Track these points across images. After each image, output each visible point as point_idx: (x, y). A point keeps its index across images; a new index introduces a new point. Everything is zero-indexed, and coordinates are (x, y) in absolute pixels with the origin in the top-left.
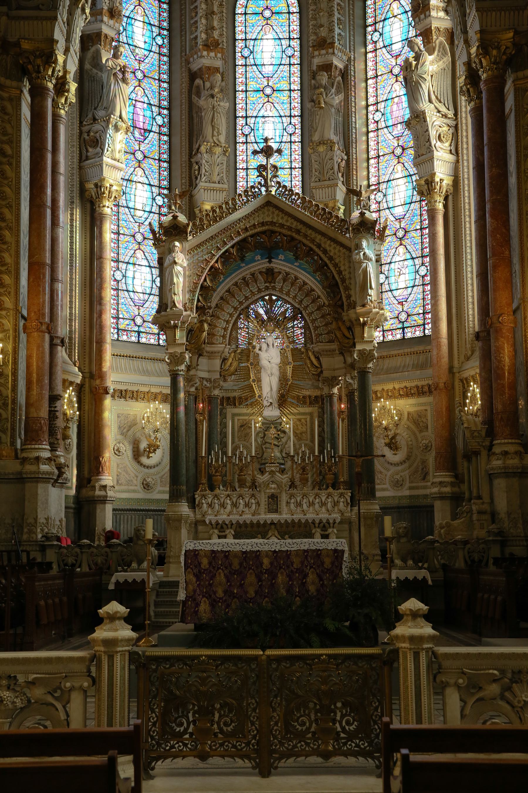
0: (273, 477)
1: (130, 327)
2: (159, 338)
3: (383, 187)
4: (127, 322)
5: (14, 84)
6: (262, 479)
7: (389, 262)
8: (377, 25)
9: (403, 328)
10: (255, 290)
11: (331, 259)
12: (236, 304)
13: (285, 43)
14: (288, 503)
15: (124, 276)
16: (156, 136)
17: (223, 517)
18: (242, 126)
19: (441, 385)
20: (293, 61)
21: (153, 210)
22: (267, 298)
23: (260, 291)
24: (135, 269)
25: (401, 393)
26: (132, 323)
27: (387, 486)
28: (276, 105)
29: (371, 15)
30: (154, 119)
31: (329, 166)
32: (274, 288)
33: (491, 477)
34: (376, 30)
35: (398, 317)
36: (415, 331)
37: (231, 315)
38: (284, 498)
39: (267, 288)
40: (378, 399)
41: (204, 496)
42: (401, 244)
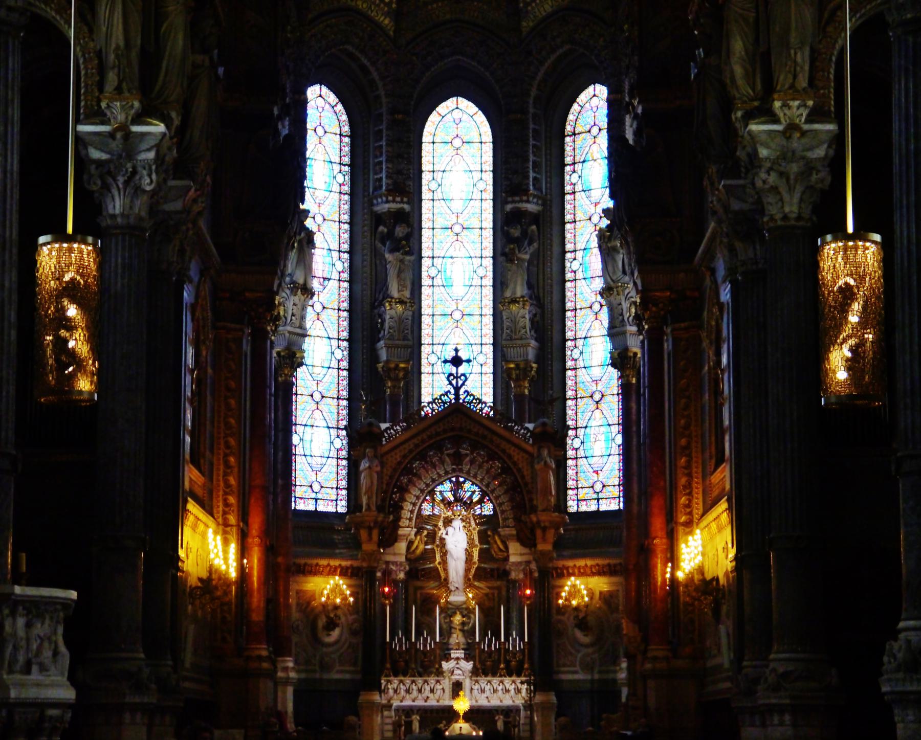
0: (457, 663)
1: (307, 494)
2: (337, 505)
3: (580, 343)
4: (304, 489)
5: (238, 326)
6: (446, 666)
7: (584, 425)
8: (576, 165)
9: (598, 500)
10: (442, 473)
11: (515, 464)
12: (423, 486)
13: (477, 175)
14: (472, 689)
15: (302, 440)
16: (336, 284)
17: (408, 702)
18: (429, 268)
19: (631, 567)
20: (484, 196)
21: (332, 366)
22: (454, 479)
23: (447, 473)
24: (313, 431)
25: (594, 570)
26: (309, 489)
27: (578, 668)
28: (465, 244)
29: (570, 154)
30: (334, 265)
31: (521, 324)
32: (461, 470)
34: (574, 171)
35: (592, 487)
36: (610, 503)
37: (418, 498)
38: (467, 683)
39: (454, 470)
40: (570, 575)
41: (389, 682)
42: (597, 408)
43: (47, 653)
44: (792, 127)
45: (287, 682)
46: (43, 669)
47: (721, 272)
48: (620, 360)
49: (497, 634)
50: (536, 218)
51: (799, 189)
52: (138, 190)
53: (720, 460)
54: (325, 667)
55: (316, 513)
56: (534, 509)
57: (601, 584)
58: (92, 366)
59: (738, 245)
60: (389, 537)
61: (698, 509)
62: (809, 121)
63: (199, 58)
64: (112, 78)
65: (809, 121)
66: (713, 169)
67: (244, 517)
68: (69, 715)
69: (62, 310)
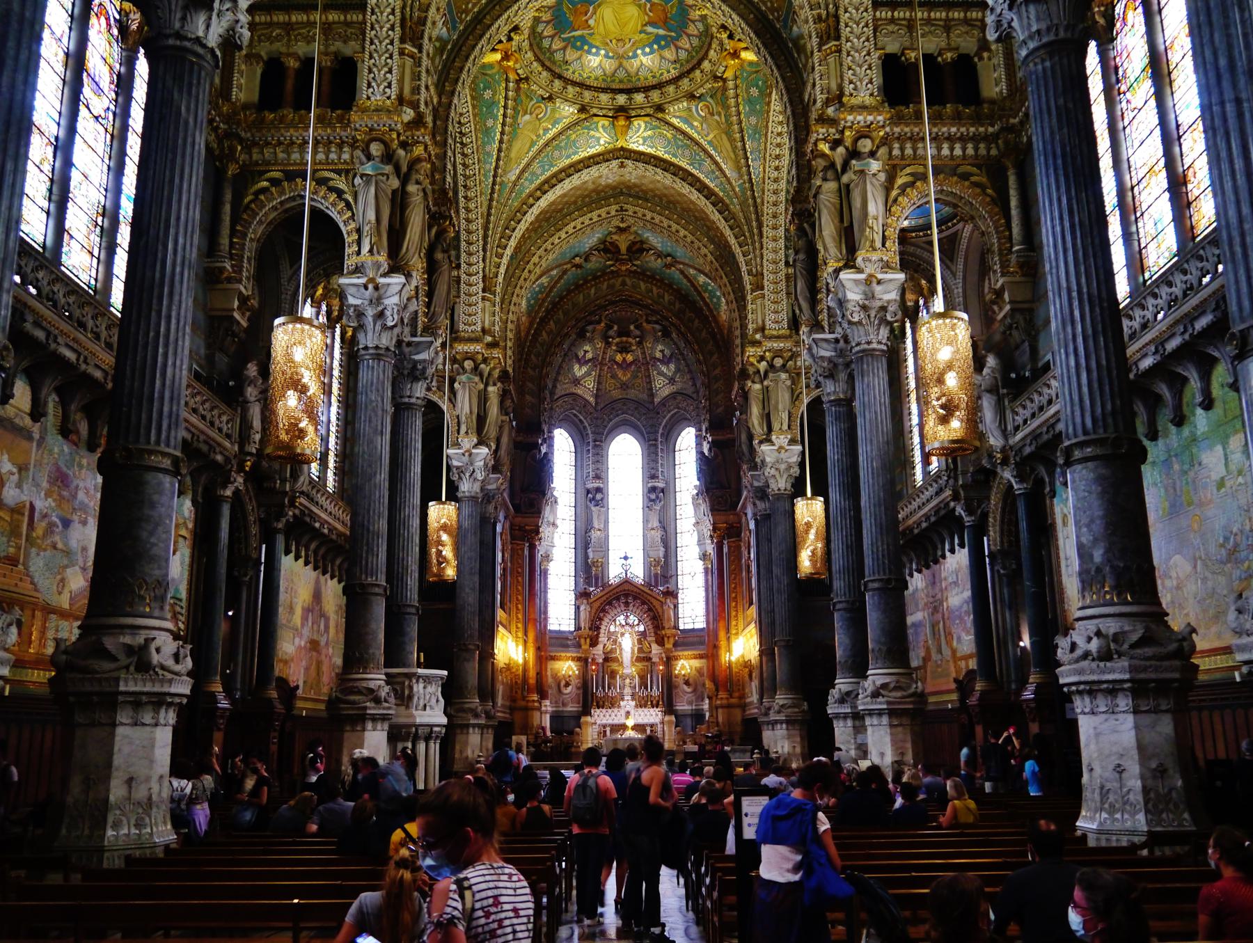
6: (622, 703)
17: (604, 722)
33: (717, 708)
38: (632, 712)
43: (434, 700)
44: (781, 447)
45: (546, 712)
46: (432, 708)
47: (750, 515)
48: (704, 557)
49: (646, 688)
50: (663, 491)
51: (785, 476)
52: (475, 479)
53: (751, 604)
54: (564, 705)
55: (559, 632)
56: (663, 628)
57: (696, 663)
58: (454, 563)
59: (758, 502)
60: (594, 642)
61: (741, 626)
62: (789, 444)
63: (506, 418)
64: (463, 429)
65: (789, 444)
66: (745, 467)
67: (526, 634)
68: (444, 730)
69: (439, 537)
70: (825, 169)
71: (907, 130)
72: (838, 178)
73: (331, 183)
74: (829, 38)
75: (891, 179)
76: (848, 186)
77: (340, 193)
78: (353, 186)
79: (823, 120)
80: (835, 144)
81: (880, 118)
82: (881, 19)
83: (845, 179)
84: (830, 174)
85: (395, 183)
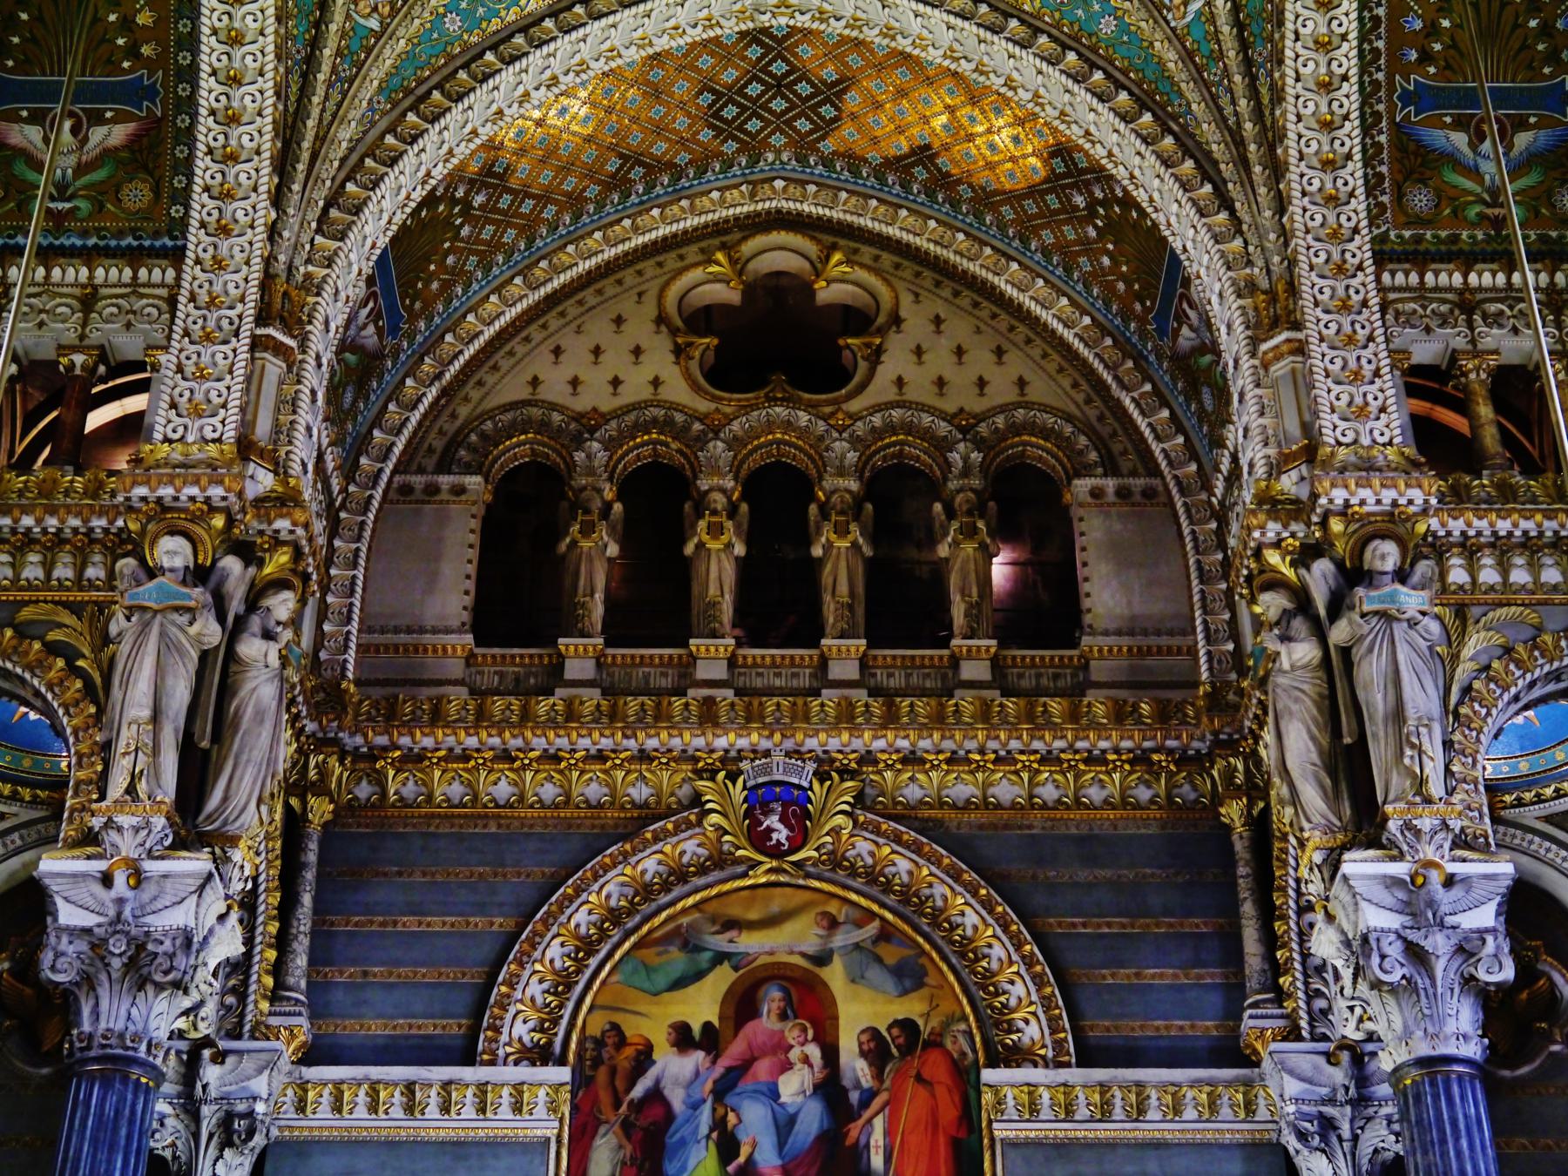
70: (1286, 616)
71: (1483, 524)
72: (1321, 636)
73: (53, 636)
74: (1275, 325)
75: (1454, 637)
76: (1346, 652)
77: (69, 653)
78: (106, 640)
79: (1270, 503)
80: (1306, 555)
81: (1417, 495)
82: (1394, 289)
83: (1339, 633)
84: (1299, 625)
85: (210, 631)
